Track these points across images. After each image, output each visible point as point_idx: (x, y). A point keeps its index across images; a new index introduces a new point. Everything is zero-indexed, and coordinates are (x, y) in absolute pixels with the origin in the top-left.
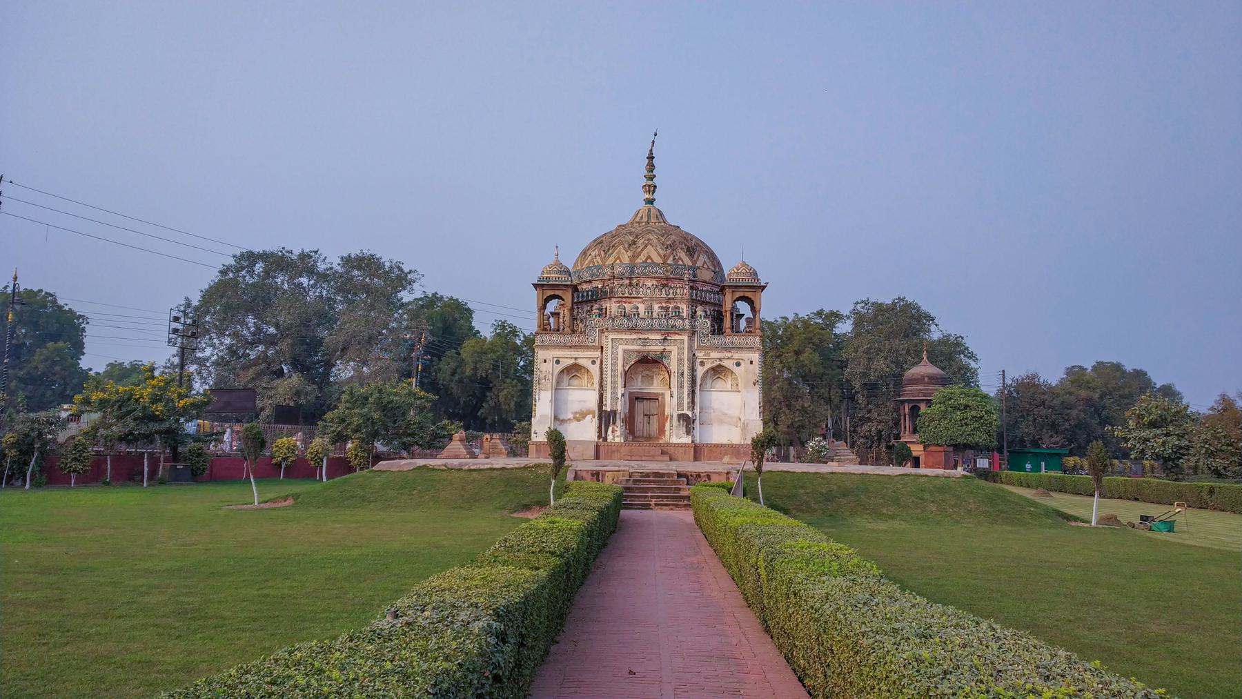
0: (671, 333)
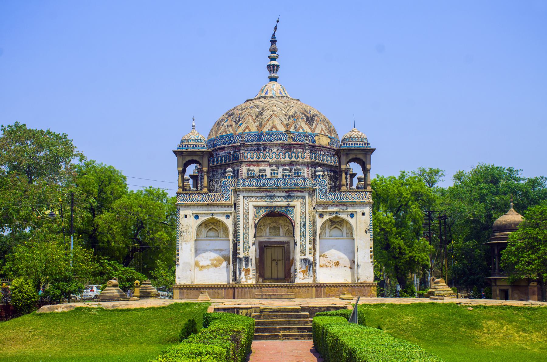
0: (294, 191)
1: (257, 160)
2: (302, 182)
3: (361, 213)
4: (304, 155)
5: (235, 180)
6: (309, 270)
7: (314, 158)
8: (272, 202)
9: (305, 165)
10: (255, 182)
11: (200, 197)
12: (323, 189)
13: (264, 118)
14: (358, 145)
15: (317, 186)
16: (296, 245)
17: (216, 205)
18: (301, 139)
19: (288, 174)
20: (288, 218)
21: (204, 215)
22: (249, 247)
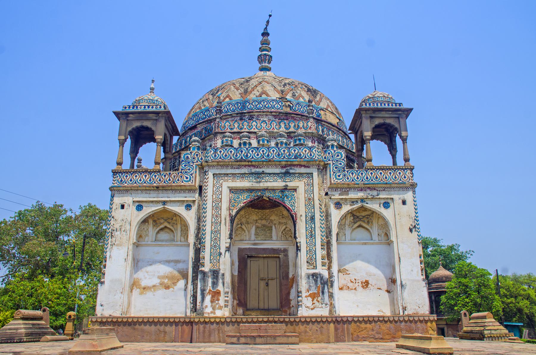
0: (294, 165)
1: (239, 131)
2: (307, 152)
3: (401, 201)
4: (307, 125)
5: (202, 153)
6: (323, 293)
7: (321, 131)
8: (260, 182)
9: (309, 138)
10: (232, 153)
11: (147, 177)
12: (340, 165)
13: (251, 84)
15: (329, 160)
16: (300, 250)
17: (171, 189)
18: (302, 110)
19: (284, 141)
20: (285, 207)
21: (151, 204)
22: (220, 254)
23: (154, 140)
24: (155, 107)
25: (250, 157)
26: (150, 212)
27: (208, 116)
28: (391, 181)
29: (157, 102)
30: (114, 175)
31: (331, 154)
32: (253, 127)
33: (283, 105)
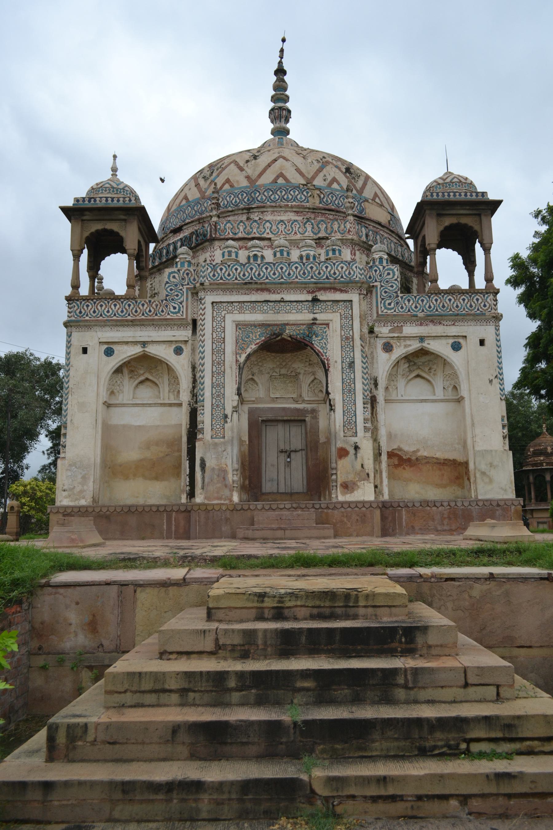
1: (246, 236)
2: (344, 270)
4: (345, 227)
11: (118, 306)
12: (391, 289)
14: (463, 196)
15: (376, 281)
18: (336, 202)
22: (226, 416)
23: (123, 251)
24: (121, 199)
25: (263, 277)
26: (125, 358)
27: (199, 213)
28: (464, 312)
29: (124, 192)
30: (69, 304)
31: (378, 272)
32: (265, 230)
33: (309, 195)
